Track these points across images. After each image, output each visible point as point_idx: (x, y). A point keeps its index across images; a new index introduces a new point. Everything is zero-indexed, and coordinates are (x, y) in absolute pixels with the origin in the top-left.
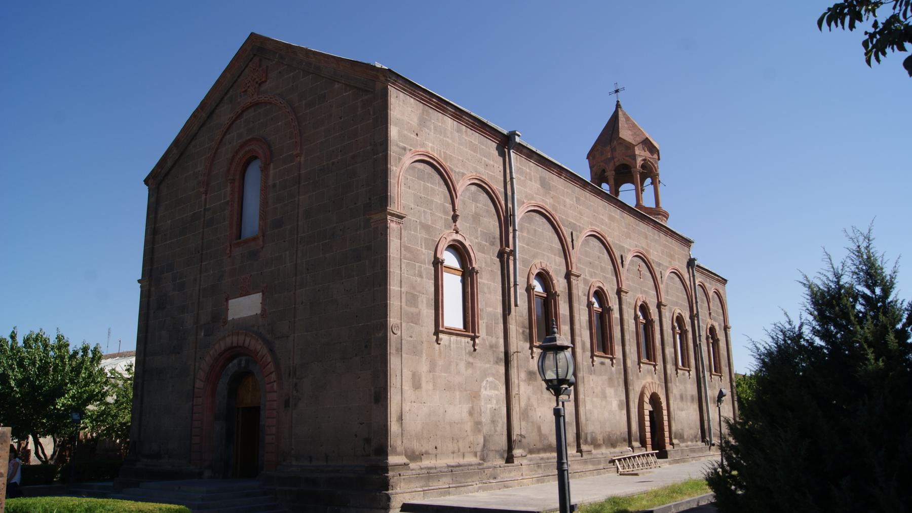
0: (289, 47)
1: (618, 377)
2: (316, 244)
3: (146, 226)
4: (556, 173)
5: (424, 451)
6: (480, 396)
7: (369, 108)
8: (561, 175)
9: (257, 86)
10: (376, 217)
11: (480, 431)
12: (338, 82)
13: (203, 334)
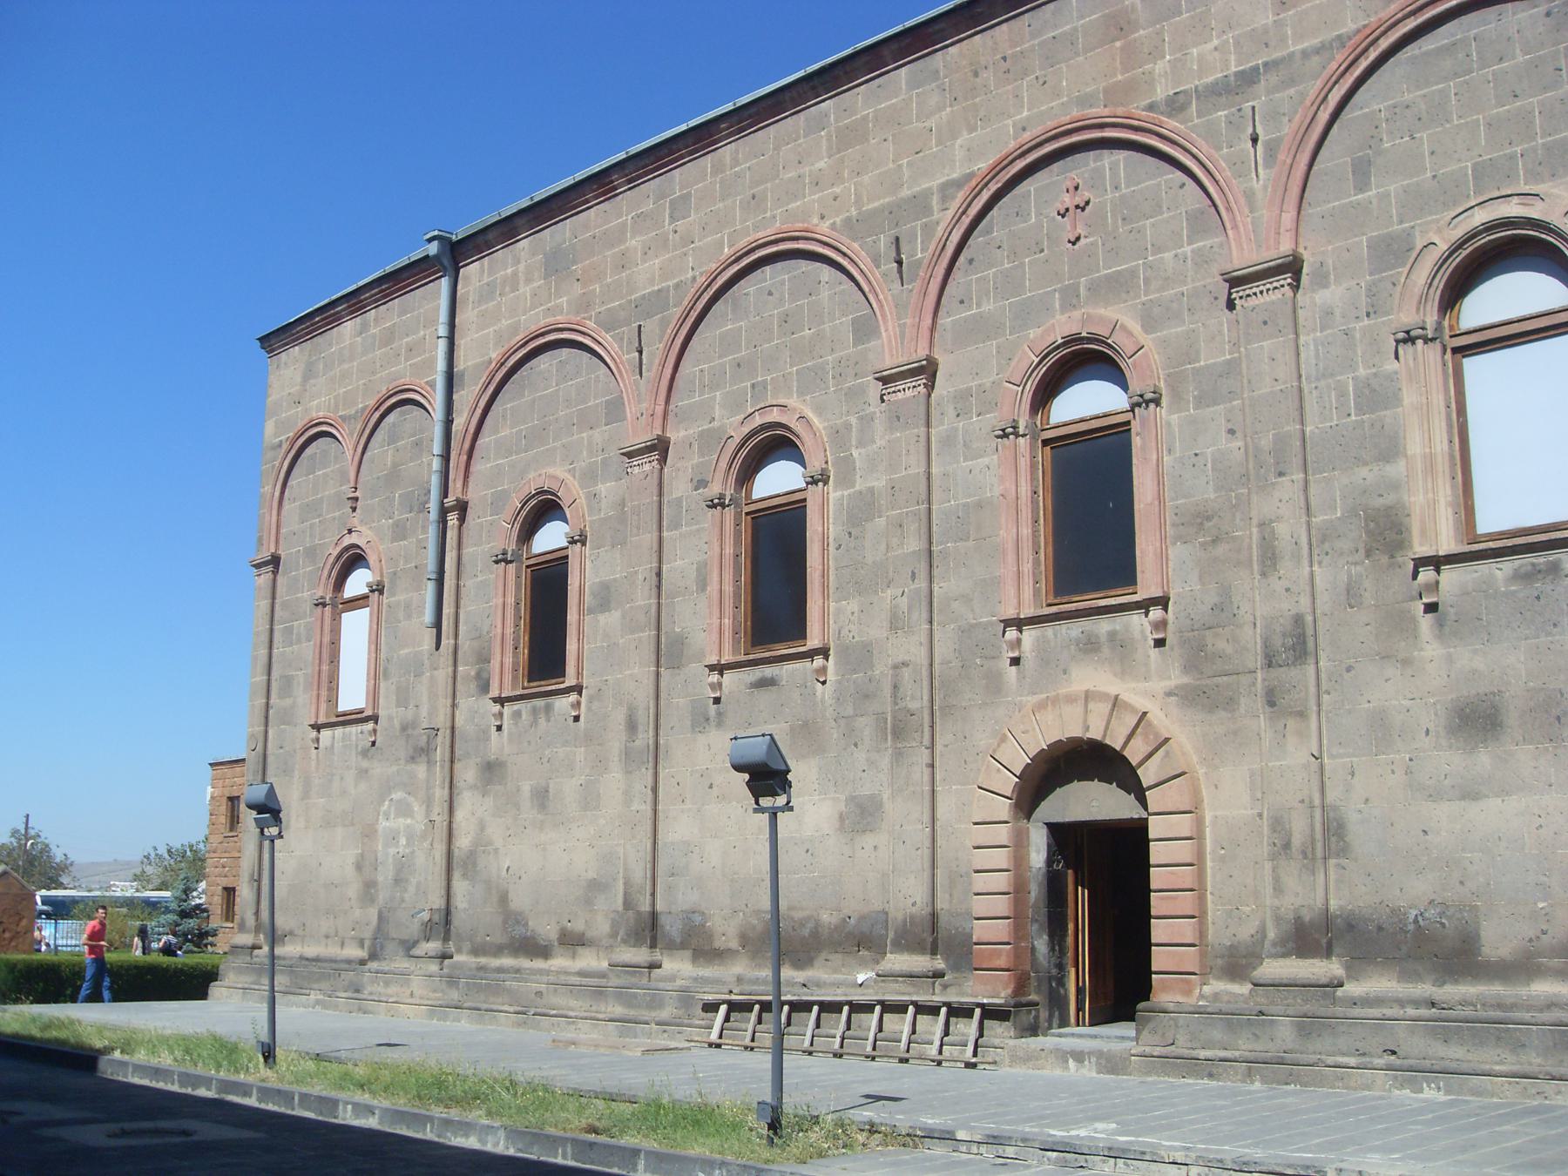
1: (850, 711)
4: (596, 197)
5: (287, 929)
6: (376, 831)
8: (615, 188)
11: (372, 901)
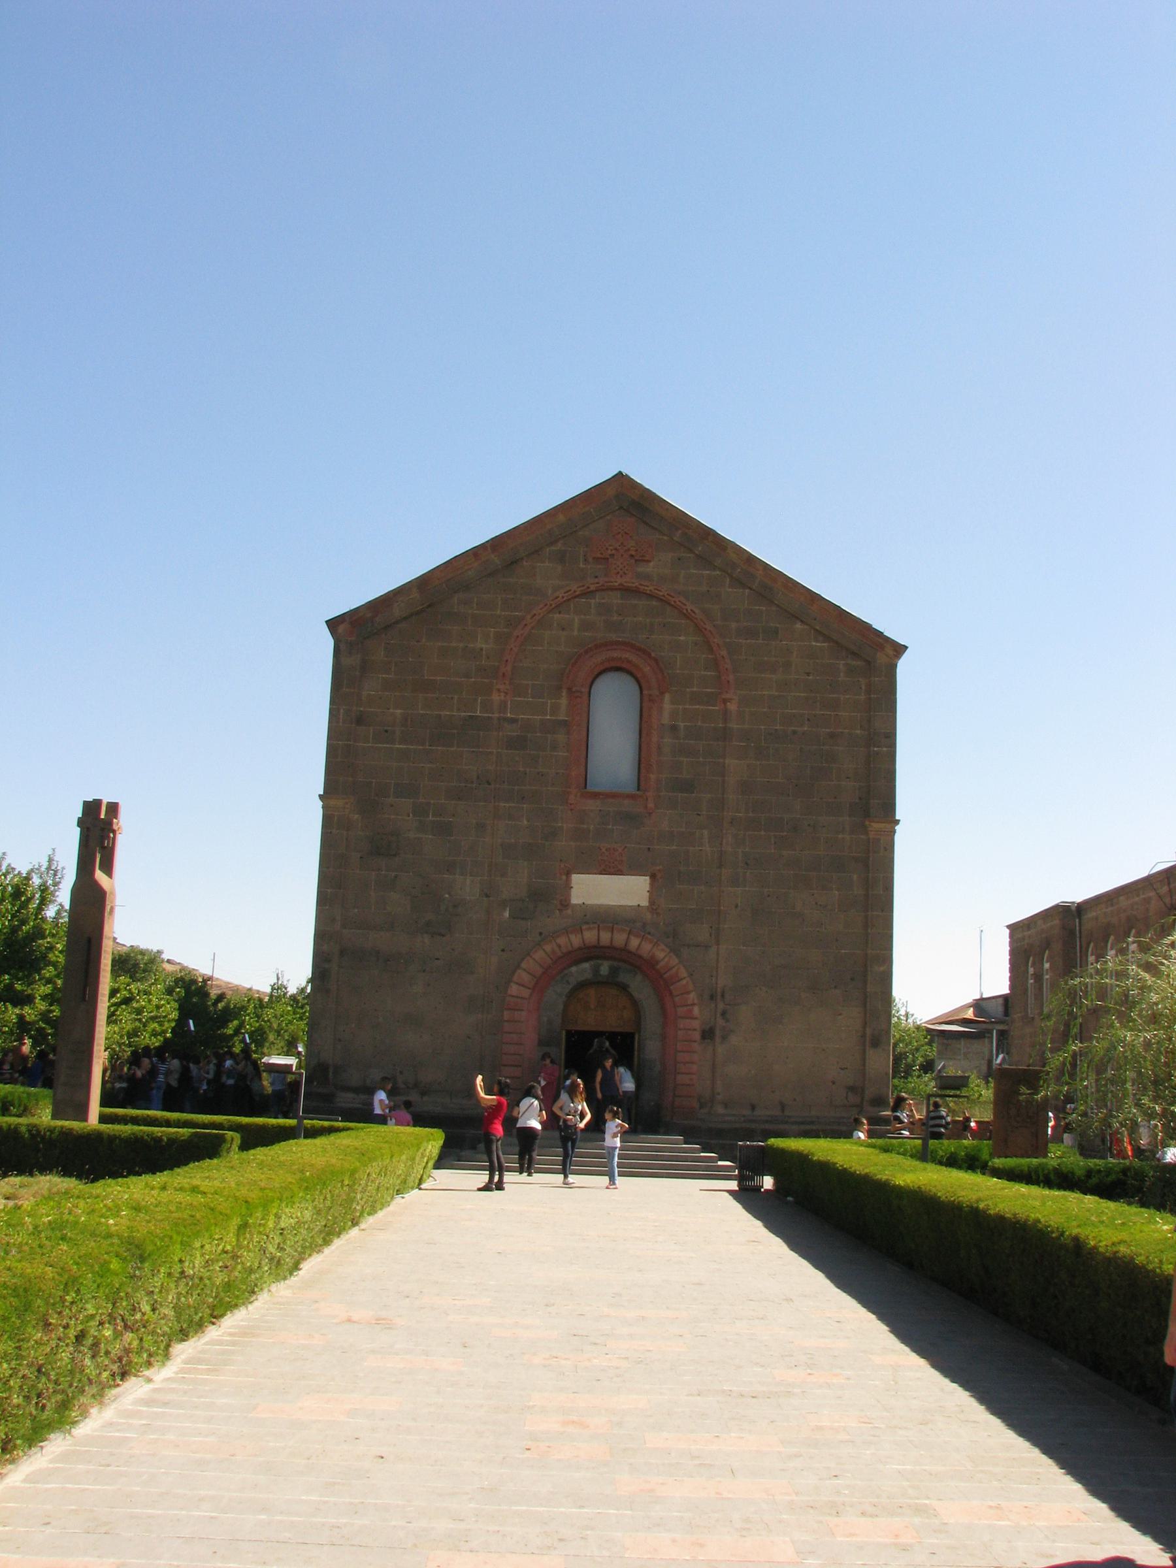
0: (708, 534)
2: (763, 833)
3: (332, 702)
7: (860, 679)
9: (633, 561)
10: (876, 826)
12: (802, 621)
13: (507, 914)
